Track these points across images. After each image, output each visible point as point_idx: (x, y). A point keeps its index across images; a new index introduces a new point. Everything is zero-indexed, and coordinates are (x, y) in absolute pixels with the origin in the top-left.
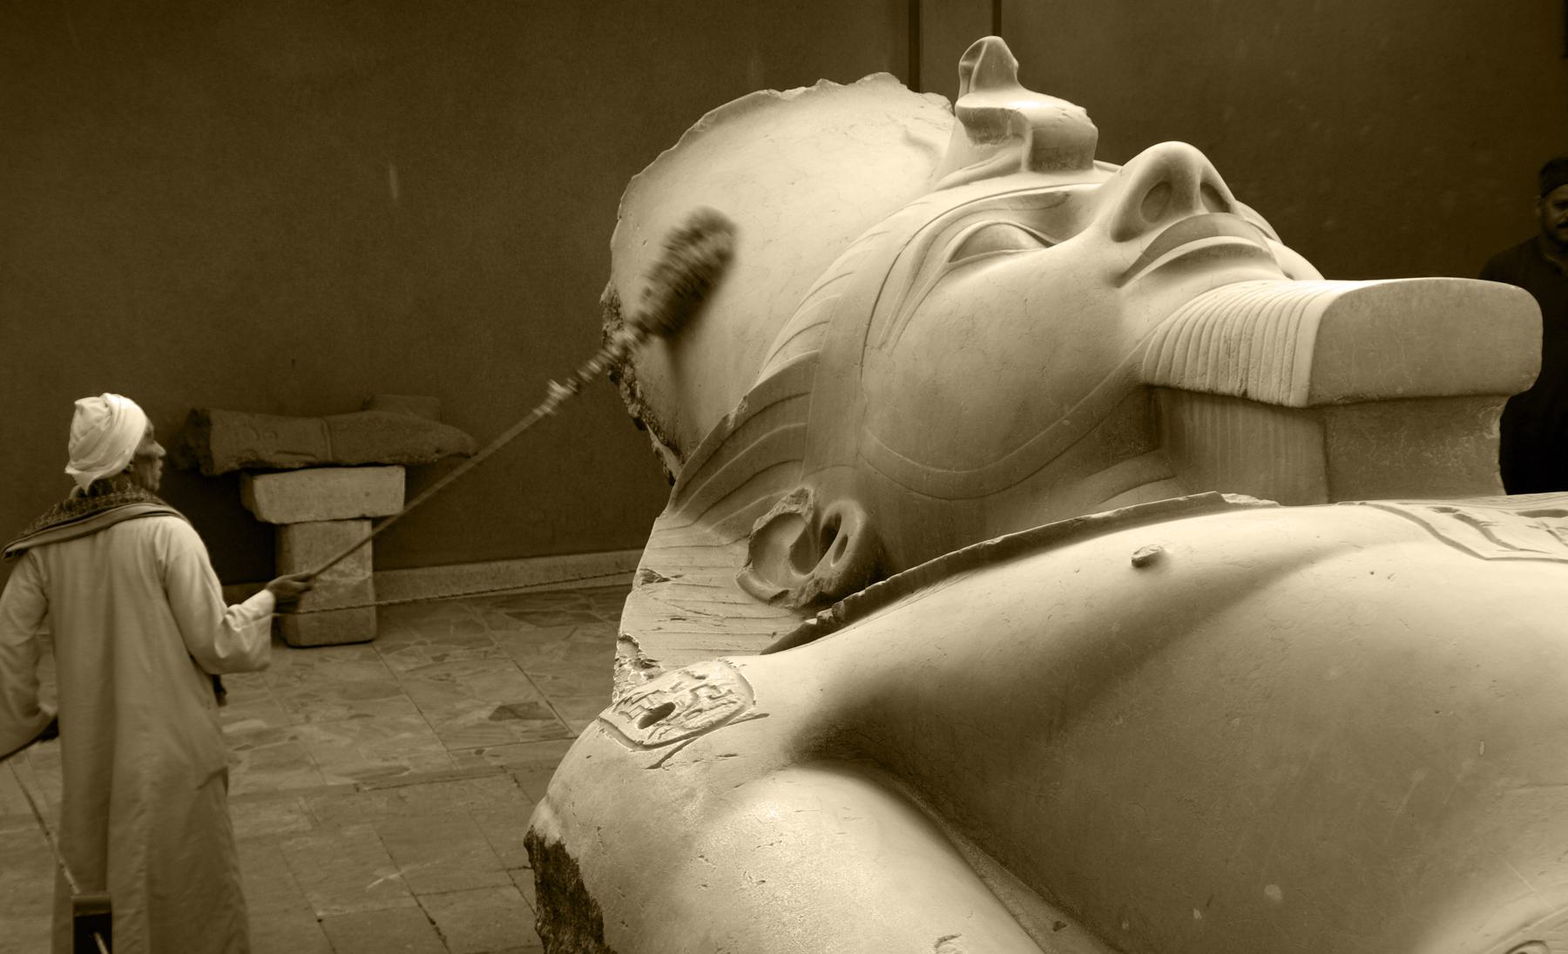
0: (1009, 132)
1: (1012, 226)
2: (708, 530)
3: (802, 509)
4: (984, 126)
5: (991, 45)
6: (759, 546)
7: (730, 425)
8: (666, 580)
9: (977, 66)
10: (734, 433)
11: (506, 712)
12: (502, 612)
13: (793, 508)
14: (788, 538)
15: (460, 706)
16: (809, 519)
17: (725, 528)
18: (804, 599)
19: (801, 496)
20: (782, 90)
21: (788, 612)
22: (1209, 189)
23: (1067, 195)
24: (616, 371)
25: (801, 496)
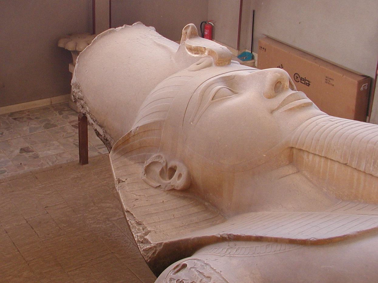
0: (206, 53)
2: (126, 159)
3: (162, 161)
4: (197, 50)
6: (147, 170)
11: (23, 150)
12: (11, 118)
13: (157, 160)
14: (157, 169)
15: (12, 149)
16: (164, 164)
17: (132, 159)
18: (167, 189)
21: (162, 192)
23: (235, 76)
25: (159, 157)
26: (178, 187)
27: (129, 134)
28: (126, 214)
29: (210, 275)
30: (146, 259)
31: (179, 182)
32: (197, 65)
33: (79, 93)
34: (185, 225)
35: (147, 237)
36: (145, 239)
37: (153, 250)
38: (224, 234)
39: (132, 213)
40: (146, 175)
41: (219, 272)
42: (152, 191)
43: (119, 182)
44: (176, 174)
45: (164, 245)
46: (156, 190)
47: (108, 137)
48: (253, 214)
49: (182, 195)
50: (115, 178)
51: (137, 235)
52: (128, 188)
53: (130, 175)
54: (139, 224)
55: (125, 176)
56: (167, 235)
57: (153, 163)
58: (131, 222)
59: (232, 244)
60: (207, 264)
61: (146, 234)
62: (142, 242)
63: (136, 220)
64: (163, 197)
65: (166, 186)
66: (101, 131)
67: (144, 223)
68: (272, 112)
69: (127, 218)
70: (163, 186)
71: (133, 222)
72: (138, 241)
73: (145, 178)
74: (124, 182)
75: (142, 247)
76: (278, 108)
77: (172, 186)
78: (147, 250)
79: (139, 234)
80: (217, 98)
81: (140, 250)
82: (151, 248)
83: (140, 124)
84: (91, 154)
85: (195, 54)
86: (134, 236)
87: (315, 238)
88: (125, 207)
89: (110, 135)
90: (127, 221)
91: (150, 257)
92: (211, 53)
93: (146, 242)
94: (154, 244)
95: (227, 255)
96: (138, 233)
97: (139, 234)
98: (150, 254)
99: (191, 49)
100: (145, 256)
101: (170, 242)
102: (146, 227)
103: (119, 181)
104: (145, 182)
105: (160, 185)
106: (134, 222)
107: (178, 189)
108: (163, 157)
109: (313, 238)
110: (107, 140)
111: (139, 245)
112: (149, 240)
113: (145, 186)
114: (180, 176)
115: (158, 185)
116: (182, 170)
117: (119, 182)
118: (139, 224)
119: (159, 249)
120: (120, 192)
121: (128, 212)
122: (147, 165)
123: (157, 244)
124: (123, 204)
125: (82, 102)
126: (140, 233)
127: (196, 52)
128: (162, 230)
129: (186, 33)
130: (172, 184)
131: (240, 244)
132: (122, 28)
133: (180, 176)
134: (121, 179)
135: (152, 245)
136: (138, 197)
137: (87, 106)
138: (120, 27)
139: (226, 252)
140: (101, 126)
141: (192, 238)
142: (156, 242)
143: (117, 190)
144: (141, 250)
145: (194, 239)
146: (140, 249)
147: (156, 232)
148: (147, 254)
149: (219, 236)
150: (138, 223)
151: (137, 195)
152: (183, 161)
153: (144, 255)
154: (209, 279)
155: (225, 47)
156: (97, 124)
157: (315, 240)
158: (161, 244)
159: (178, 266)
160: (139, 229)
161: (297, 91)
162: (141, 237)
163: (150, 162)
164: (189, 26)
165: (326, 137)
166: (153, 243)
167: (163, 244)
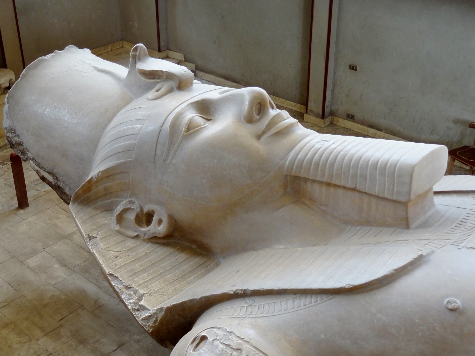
1: (192, 115)
3: (134, 206)
4: (153, 75)
5: (141, 47)
6: (120, 219)
7: (94, 179)
8: (96, 237)
9: (138, 53)
10: (96, 182)
13: (129, 206)
14: (131, 216)
16: (139, 210)
17: (96, 208)
18: (146, 237)
19: (131, 202)
20: (45, 56)
21: (142, 241)
22: (270, 103)
24: (16, 148)
26: (159, 234)
27: (90, 181)
28: (109, 278)
29: (240, 347)
30: (147, 330)
31: (159, 228)
33: (16, 138)
34: (178, 277)
35: (142, 303)
36: (141, 306)
37: (153, 317)
38: (237, 290)
39: (116, 275)
41: (249, 340)
42: (131, 243)
43: (90, 239)
44: (155, 219)
45: (165, 310)
46: (134, 241)
47: (62, 185)
48: (253, 254)
49: (165, 241)
50: (84, 234)
51: (130, 303)
52: (102, 246)
53: (100, 227)
54: (128, 288)
55: (95, 229)
56: (164, 295)
57: (126, 210)
58: (118, 288)
59: (249, 301)
60: (231, 332)
61: (140, 299)
62: (138, 310)
63: (124, 284)
64: (145, 248)
65: (145, 235)
66: (50, 178)
67: (133, 285)
68: (259, 137)
69: (112, 283)
70: (142, 235)
71: (121, 287)
72: (134, 310)
73: (118, 228)
74: (96, 237)
75: (139, 316)
76: (264, 133)
77: (154, 233)
78: (147, 319)
79: (131, 301)
80: (191, 129)
81: (138, 320)
82: (150, 316)
83: (102, 168)
84: (30, 194)
85: (151, 79)
86: (127, 304)
87: (351, 285)
88: (107, 270)
89: (64, 182)
90: (112, 287)
91: (152, 327)
92: (169, 76)
93: (142, 308)
94: (153, 310)
95: (249, 316)
96: (130, 299)
97: (131, 301)
98: (151, 323)
100: (145, 326)
101: (173, 306)
102: (137, 290)
103: (90, 238)
104: (119, 232)
105: (138, 235)
106: (122, 286)
107: (161, 236)
108: (136, 202)
109: (348, 286)
110: (59, 187)
111: (135, 314)
112: (146, 306)
113: (120, 238)
114: (160, 222)
115: (136, 234)
116: (161, 213)
117: (90, 239)
118: (128, 288)
119: (160, 316)
120: (95, 252)
121: (112, 275)
122: (118, 213)
123: (157, 310)
124: (103, 266)
125: (21, 148)
126: (132, 299)
127: (151, 77)
128: (156, 290)
129: (136, 55)
130: (152, 231)
131: (259, 301)
132: (53, 55)
133: (160, 222)
134: (91, 234)
135: (151, 312)
136: (117, 254)
137: (29, 152)
138: (51, 54)
139: (246, 311)
140: (50, 173)
141: (199, 297)
142: (154, 307)
143: (91, 250)
144: (139, 320)
145: (201, 298)
146: (137, 318)
147: (150, 295)
148: (147, 323)
149: (232, 293)
150: (126, 287)
151: (115, 252)
152: (160, 203)
153: (144, 325)
154: (240, 351)
155: (185, 68)
156: (45, 171)
157: (351, 287)
158: (161, 309)
159: (195, 339)
160: (130, 295)
161: (278, 111)
162: (135, 304)
163: (121, 209)
164: (137, 47)
165: (327, 161)
166: (152, 309)
167: (164, 309)
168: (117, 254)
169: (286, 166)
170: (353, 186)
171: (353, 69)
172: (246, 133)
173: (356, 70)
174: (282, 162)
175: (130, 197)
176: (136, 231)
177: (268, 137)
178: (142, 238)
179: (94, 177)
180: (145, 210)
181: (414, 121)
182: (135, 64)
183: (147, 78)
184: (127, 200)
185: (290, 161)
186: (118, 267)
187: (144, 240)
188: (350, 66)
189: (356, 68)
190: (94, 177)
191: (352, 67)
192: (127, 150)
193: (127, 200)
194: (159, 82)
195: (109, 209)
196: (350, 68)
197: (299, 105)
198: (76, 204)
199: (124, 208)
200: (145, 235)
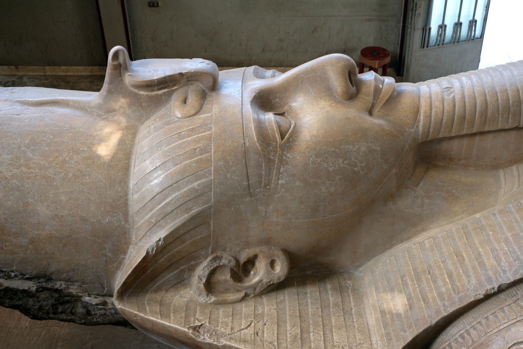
3: (224, 261)
13: (215, 265)
14: (225, 276)
16: (233, 263)
18: (258, 291)
21: (253, 299)
25: (215, 259)
32: (185, 103)
38: (487, 290)
40: (210, 294)
42: (246, 308)
46: (243, 304)
50: (186, 330)
57: (213, 273)
73: (213, 299)
77: (270, 282)
85: (159, 90)
99: (150, 85)
103: (196, 329)
105: (246, 293)
115: (242, 294)
122: (204, 280)
133: (272, 264)
168: (251, 330)
169: (421, 132)
170: (516, 125)
171: (154, 6)
172: (353, 113)
173: (158, 6)
174: (412, 130)
175: (212, 253)
176: (238, 291)
177: (381, 108)
178: (252, 295)
179: (150, 250)
180: (243, 258)
181: (241, 45)
182: (120, 76)
183: (152, 91)
184: (209, 259)
185: (424, 125)
186: (276, 344)
187: (255, 296)
188: (149, 3)
189: (157, 3)
190: (150, 250)
191: (151, 5)
192: (197, 196)
193: (209, 259)
194: (176, 90)
195: (181, 282)
196: (150, 6)
197: (90, 67)
198: (125, 298)
199: (210, 269)
200: (255, 289)
